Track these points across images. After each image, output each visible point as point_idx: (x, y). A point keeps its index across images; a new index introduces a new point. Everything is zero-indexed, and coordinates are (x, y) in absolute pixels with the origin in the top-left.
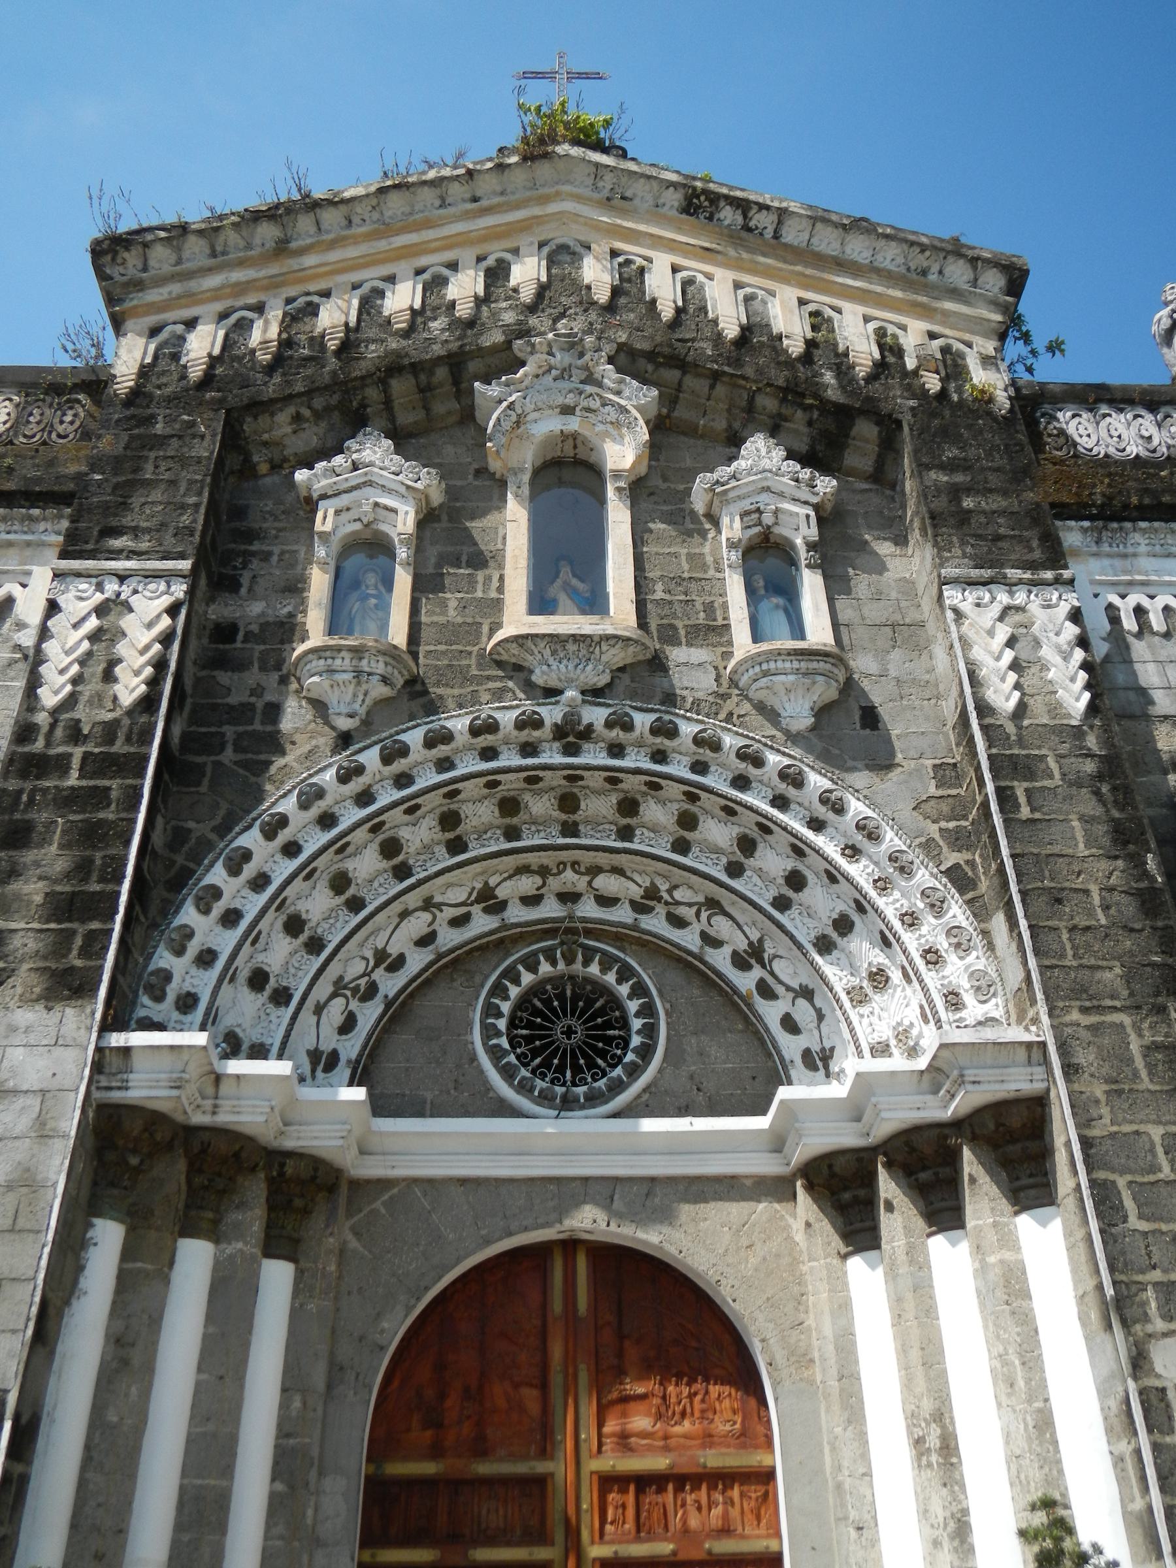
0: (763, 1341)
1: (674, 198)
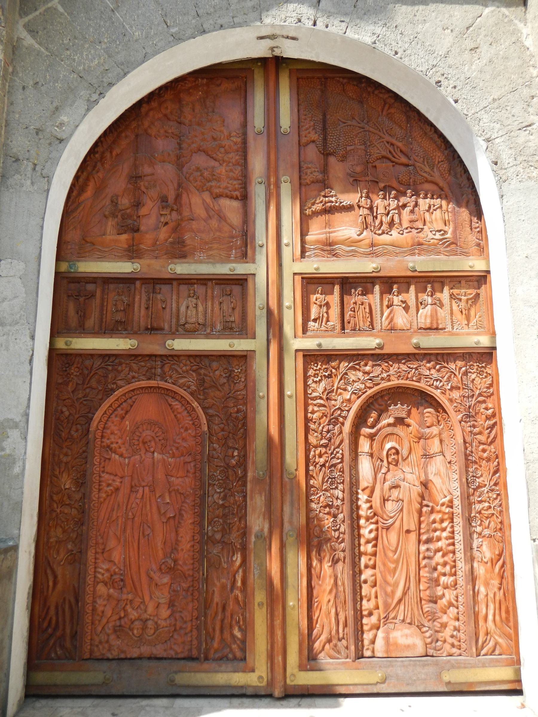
0: (488, 140)
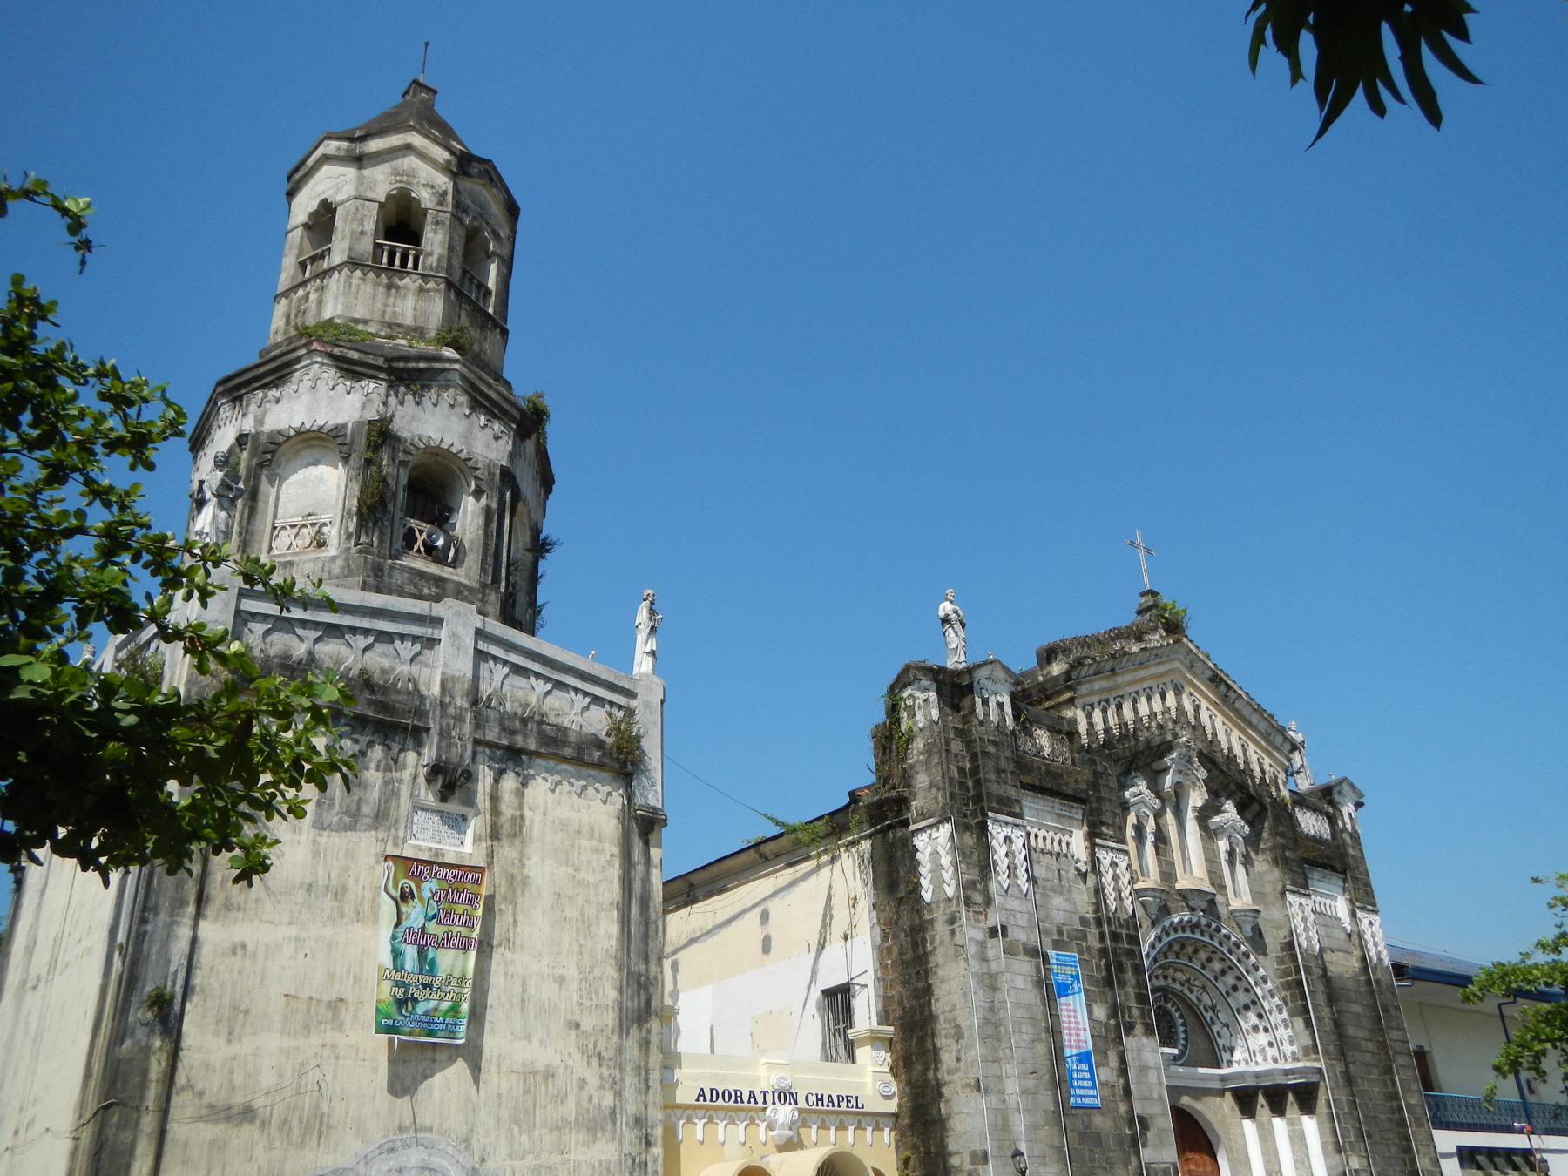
1: (1209, 674)
